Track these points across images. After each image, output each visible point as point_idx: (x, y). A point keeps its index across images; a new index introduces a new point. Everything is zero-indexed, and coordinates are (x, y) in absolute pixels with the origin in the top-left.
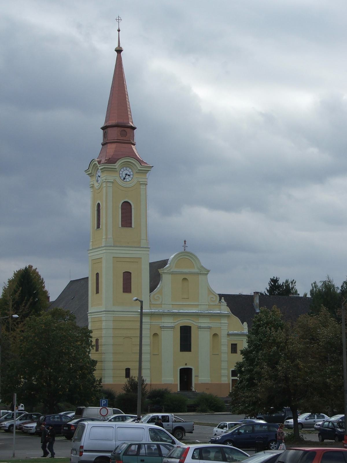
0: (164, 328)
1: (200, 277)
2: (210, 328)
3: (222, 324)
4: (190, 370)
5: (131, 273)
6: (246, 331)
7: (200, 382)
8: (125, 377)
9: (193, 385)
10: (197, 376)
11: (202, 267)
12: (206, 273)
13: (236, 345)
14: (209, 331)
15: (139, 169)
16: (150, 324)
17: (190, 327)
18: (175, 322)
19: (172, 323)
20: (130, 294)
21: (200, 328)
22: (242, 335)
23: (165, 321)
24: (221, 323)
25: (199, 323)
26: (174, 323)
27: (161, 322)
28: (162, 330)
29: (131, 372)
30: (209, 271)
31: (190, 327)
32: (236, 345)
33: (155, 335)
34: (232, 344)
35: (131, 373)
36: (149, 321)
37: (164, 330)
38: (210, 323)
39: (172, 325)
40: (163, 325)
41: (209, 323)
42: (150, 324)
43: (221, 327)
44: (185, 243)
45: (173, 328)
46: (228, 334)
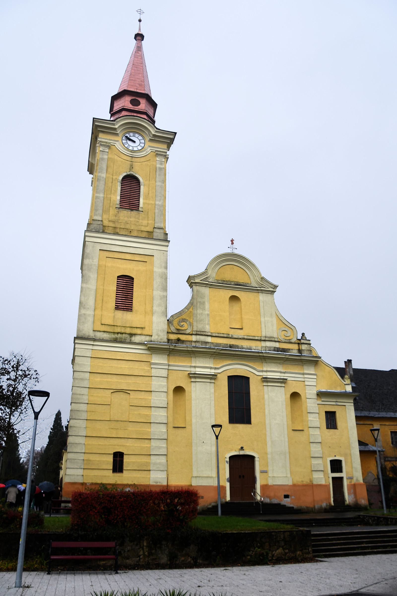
0: (195, 378)
1: (262, 297)
2: (284, 381)
3: (306, 376)
5: (133, 279)
6: (349, 389)
7: (270, 482)
8: (112, 471)
9: (258, 490)
10: (266, 472)
11: (262, 278)
12: (272, 290)
15: (153, 133)
16: (167, 367)
17: (247, 379)
18: (218, 369)
19: (211, 368)
20: (129, 313)
21: (265, 380)
23: (197, 365)
25: (262, 371)
26: (216, 368)
27: (191, 367)
28: (193, 380)
29: (124, 460)
30: (276, 287)
31: (247, 379)
33: (179, 390)
34: (326, 412)
35: (124, 464)
36: (166, 362)
37: (195, 382)
38: (284, 373)
39: (213, 372)
40: (193, 370)
41: (281, 372)
42: (167, 367)
43: (304, 381)
44: (232, 243)
45: (213, 377)
46: (317, 394)
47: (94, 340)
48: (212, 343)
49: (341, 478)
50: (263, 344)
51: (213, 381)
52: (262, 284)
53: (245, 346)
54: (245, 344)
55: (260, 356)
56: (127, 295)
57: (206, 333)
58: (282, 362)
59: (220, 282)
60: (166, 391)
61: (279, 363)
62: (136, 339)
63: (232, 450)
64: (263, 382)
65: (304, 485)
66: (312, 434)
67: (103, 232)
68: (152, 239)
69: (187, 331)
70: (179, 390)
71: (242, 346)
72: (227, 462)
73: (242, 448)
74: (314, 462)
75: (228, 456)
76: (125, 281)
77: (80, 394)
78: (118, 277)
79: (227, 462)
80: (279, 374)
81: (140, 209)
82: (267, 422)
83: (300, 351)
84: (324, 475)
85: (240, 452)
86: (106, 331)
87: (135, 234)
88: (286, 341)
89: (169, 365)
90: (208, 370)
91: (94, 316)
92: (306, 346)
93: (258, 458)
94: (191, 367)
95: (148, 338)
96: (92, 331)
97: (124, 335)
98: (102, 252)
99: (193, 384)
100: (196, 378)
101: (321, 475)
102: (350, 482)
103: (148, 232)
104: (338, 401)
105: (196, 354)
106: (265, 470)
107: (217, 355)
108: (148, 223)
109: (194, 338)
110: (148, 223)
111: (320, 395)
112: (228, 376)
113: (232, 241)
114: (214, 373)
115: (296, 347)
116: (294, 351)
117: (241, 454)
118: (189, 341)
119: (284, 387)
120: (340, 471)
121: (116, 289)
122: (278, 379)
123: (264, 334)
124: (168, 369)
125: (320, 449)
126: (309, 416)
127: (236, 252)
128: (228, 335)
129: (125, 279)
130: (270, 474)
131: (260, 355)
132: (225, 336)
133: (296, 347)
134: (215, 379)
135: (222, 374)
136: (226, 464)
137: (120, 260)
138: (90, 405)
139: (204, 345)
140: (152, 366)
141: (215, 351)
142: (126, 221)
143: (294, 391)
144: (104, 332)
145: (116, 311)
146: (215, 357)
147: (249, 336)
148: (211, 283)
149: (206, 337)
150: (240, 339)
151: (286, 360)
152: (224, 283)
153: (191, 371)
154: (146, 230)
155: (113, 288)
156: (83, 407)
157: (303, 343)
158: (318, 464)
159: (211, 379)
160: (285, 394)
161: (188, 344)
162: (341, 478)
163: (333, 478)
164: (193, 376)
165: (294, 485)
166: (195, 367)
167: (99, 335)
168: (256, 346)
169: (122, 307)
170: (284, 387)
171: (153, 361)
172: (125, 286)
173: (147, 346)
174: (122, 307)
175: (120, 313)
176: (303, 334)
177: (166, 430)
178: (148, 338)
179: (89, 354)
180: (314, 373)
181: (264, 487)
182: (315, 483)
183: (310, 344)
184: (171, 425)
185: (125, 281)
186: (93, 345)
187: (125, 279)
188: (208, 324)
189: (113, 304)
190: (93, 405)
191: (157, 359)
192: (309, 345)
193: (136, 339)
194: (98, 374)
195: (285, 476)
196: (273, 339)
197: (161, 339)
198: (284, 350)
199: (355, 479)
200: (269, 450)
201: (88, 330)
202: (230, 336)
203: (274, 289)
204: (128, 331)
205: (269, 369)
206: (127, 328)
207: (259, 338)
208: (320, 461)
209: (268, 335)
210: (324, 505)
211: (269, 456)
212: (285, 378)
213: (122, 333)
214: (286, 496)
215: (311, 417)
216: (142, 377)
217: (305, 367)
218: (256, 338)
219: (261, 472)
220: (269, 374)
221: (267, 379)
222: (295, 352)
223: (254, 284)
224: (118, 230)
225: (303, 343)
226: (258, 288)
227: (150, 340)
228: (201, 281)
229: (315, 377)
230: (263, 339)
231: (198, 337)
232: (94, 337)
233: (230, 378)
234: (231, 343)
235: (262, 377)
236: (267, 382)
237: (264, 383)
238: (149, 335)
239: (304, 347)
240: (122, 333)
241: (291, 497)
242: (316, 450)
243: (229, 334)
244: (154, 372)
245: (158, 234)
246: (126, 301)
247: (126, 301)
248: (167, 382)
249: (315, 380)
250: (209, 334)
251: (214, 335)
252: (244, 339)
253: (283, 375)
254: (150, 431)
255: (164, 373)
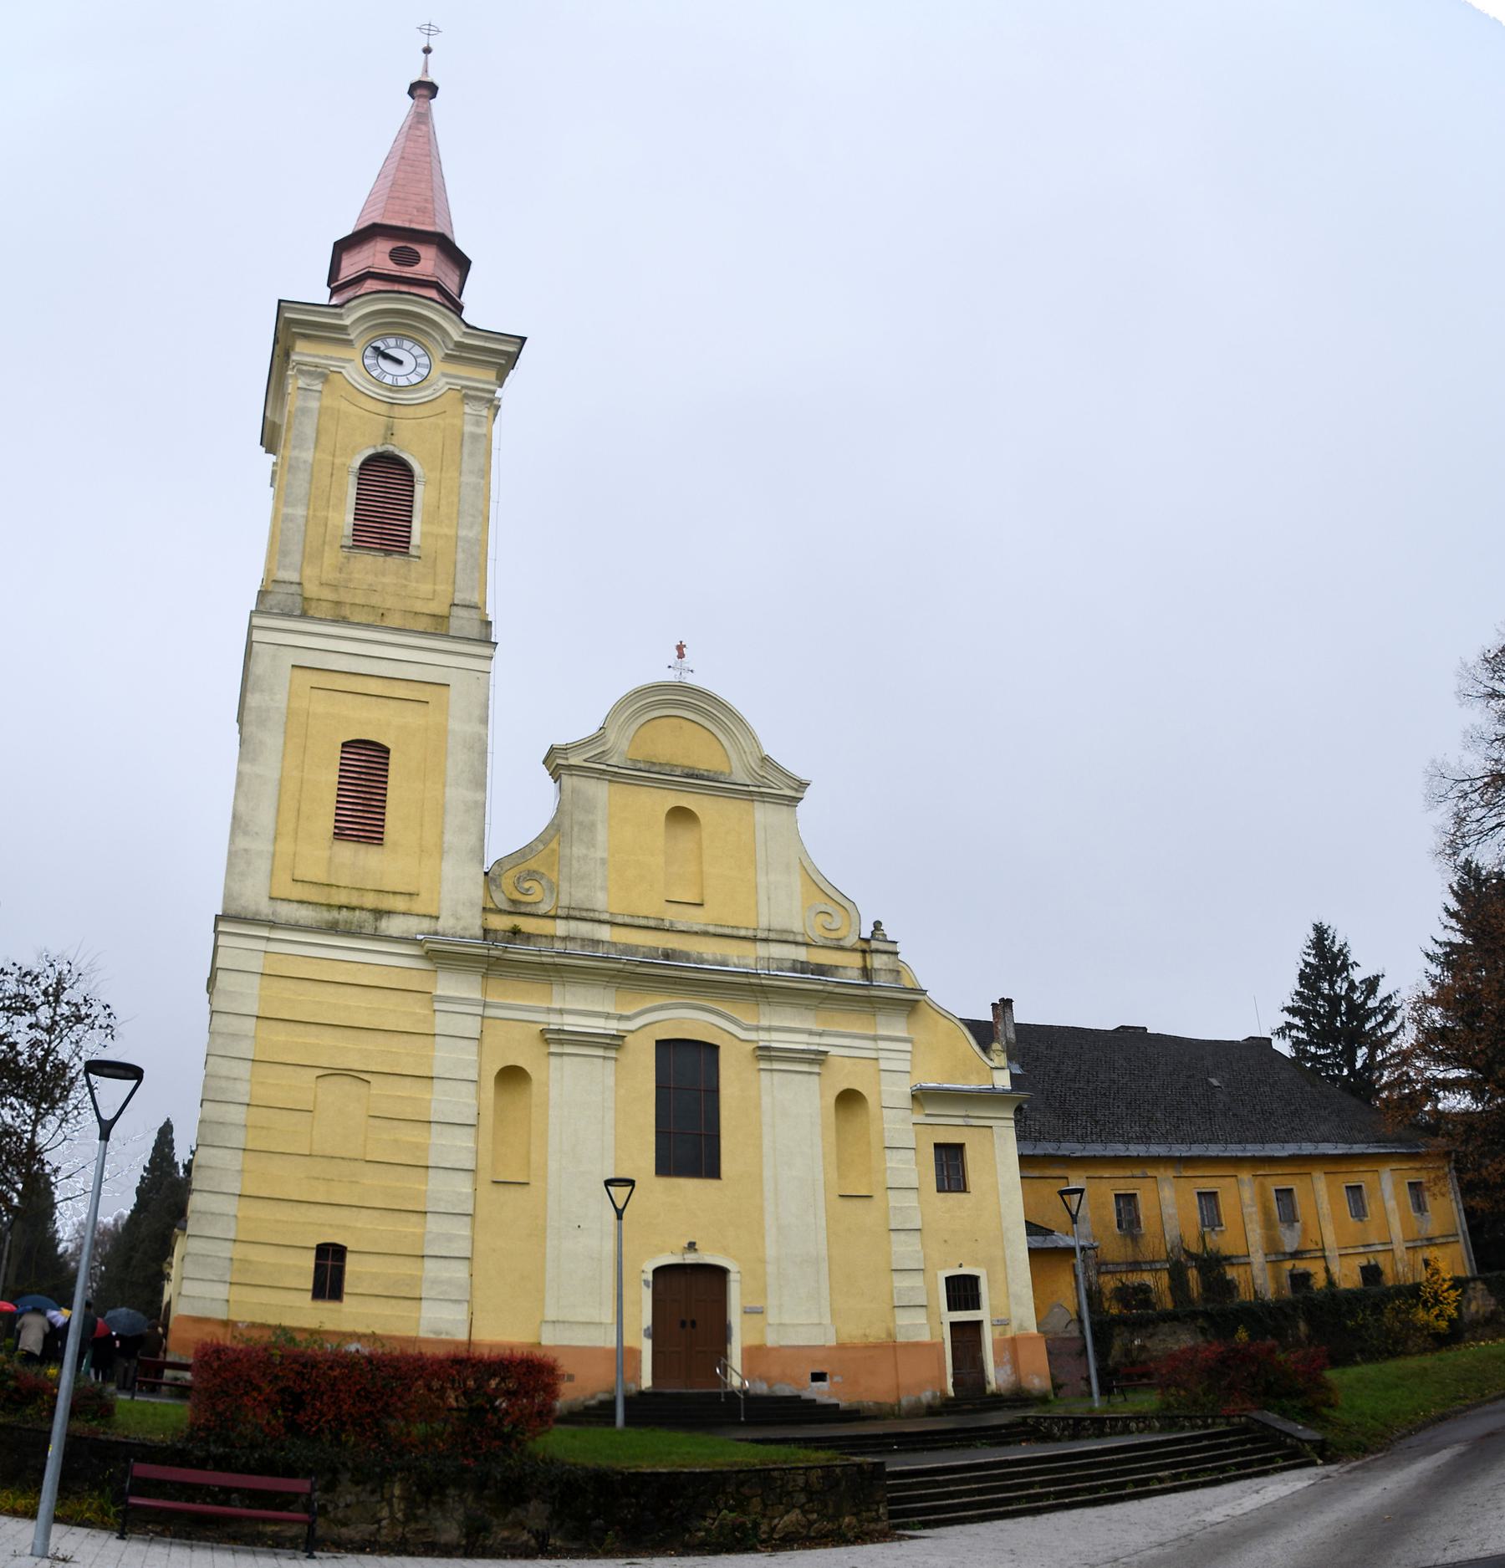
0: (560, 1042)
1: (763, 814)
2: (818, 1058)
4: (718, 1274)
5: (387, 751)
6: (1003, 1081)
7: (772, 1340)
10: (760, 1311)
11: (765, 760)
13: (959, 1148)
14: (816, 1078)
16: (479, 1010)
17: (714, 1049)
18: (628, 1018)
19: (608, 1016)
20: (373, 850)
21: (765, 1053)
22: (987, 1098)
23: (568, 1006)
24: (875, 1038)
25: (758, 1029)
26: (621, 1018)
27: (549, 1010)
28: (554, 1049)
30: (803, 785)
31: (714, 1049)
32: (959, 1148)
33: (512, 1076)
37: (561, 1055)
38: (820, 1034)
39: (612, 1027)
40: (555, 1021)
41: (811, 1033)
42: (479, 1010)
43: (877, 1059)
44: (681, 656)
45: (614, 1042)
46: (913, 1095)
47: (273, 925)
48: (614, 944)
49: (977, 1325)
50: (763, 950)
51: (612, 1054)
52: (763, 777)
53: (707, 954)
54: (709, 949)
55: (751, 984)
56: (368, 796)
57: (596, 916)
58: (815, 1002)
59: (641, 766)
60: (476, 1078)
61: (807, 1007)
62: (393, 926)
63: (662, 1250)
64: (760, 1058)
65: (867, 1347)
66: (895, 1208)
67: (304, 615)
68: (446, 636)
69: (541, 905)
70: (512, 1076)
71: (701, 954)
72: (646, 1282)
73: (692, 1246)
74: (902, 1282)
75: (650, 1266)
76: (363, 758)
77: (228, 1078)
78: (344, 745)
79: (646, 1282)
80: (804, 1038)
81: (413, 551)
82: (767, 1173)
83: (866, 972)
84: (928, 1319)
85: (686, 1256)
86: (305, 899)
87: (395, 620)
88: (829, 943)
89: (485, 1005)
90: (600, 1022)
91: (274, 855)
92: (885, 957)
93: (739, 1272)
94: (549, 1010)
95: (426, 924)
96: (266, 899)
97: (357, 912)
98: (298, 672)
99: (553, 1060)
100: (562, 1044)
101: (920, 1317)
102: (1001, 1335)
103: (434, 616)
104: (970, 1114)
105: (564, 975)
106: (758, 1305)
107: (627, 978)
108: (434, 591)
109: (561, 928)
110: (434, 591)
111: (922, 1097)
112: (657, 1042)
113: (680, 648)
114: (617, 1030)
115: (856, 960)
116: (849, 973)
117: (688, 1261)
118: (546, 936)
119: (819, 1074)
120: (975, 1304)
121: (336, 779)
122: (803, 1051)
123: (764, 923)
124: (483, 1017)
125: (919, 1247)
126: (887, 1157)
127: (691, 680)
128: (660, 922)
129: (363, 752)
130: (772, 1317)
131: (752, 980)
132: (652, 923)
133: (856, 960)
134: (618, 1048)
135: (639, 1034)
136: (644, 1288)
137: (350, 696)
138: (254, 1109)
139: (591, 949)
140: (437, 1006)
141: (621, 966)
142: (371, 585)
143: (846, 1086)
144: (301, 902)
145: (338, 843)
146: (620, 983)
147: (721, 926)
148: (616, 770)
149: (596, 926)
150: (696, 933)
151: (826, 998)
152: (653, 769)
153: (549, 1024)
154: (428, 612)
155: (327, 777)
156: (236, 1114)
157: (877, 951)
158: (913, 1288)
159: (607, 1047)
160: (822, 1096)
161: (543, 944)
162: (977, 1325)
163: (953, 1325)
164: (553, 1038)
165: (841, 1347)
166: (561, 1012)
167: (287, 912)
168: (741, 957)
169: (355, 833)
170: (819, 1074)
171: (439, 992)
172: (364, 770)
173: (422, 946)
174: (355, 833)
175: (347, 851)
176: (877, 925)
177: (470, 1190)
178: (426, 924)
179: (256, 964)
180: (905, 1035)
181: (754, 1353)
182: (900, 1339)
183: (897, 953)
184: (486, 1176)
185: (363, 758)
186: (268, 939)
187: (363, 752)
188: (604, 888)
189: (328, 824)
190: (264, 1109)
191: (450, 985)
192: (892, 957)
193: (393, 926)
194: (281, 1024)
195: (818, 1322)
196: (791, 938)
197: (465, 929)
198: (821, 970)
199: (1014, 1324)
200: (771, 1251)
201: (255, 899)
202: (667, 925)
203: (796, 790)
204: (370, 901)
205: (776, 1023)
206: (366, 893)
207: (750, 933)
208: (917, 1281)
209: (776, 925)
210: (926, 1396)
211: (771, 1269)
212: (822, 1048)
213: (353, 909)
214: (818, 1377)
215: (894, 1160)
216: (405, 1037)
217: (881, 1019)
218: (742, 933)
219: (745, 1312)
220: (775, 1036)
221: (770, 1051)
222: (854, 977)
223: (740, 776)
224: (346, 611)
225: (877, 951)
226: (751, 789)
227: (432, 930)
228: (585, 761)
229: (908, 1047)
230: (761, 935)
231: (573, 924)
232: (271, 918)
233: (662, 1045)
234: (670, 946)
235: (755, 1045)
236: (770, 1059)
237: (761, 1062)
238: (431, 917)
239: (878, 961)
240: (353, 909)
241: (831, 1378)
242: (906, 1250)
243: (663, 920)
244: (442, 1023)
245: (463, 622)
246: (366, 815)
247: (366, 815)
248: (480, 1054)
249: (908, 1056)
250: (605, 917)
251: (619, 920)
252: (706, 934)
253: (816, 1039)
254: (426, 1191)
255: (471, 1026)
